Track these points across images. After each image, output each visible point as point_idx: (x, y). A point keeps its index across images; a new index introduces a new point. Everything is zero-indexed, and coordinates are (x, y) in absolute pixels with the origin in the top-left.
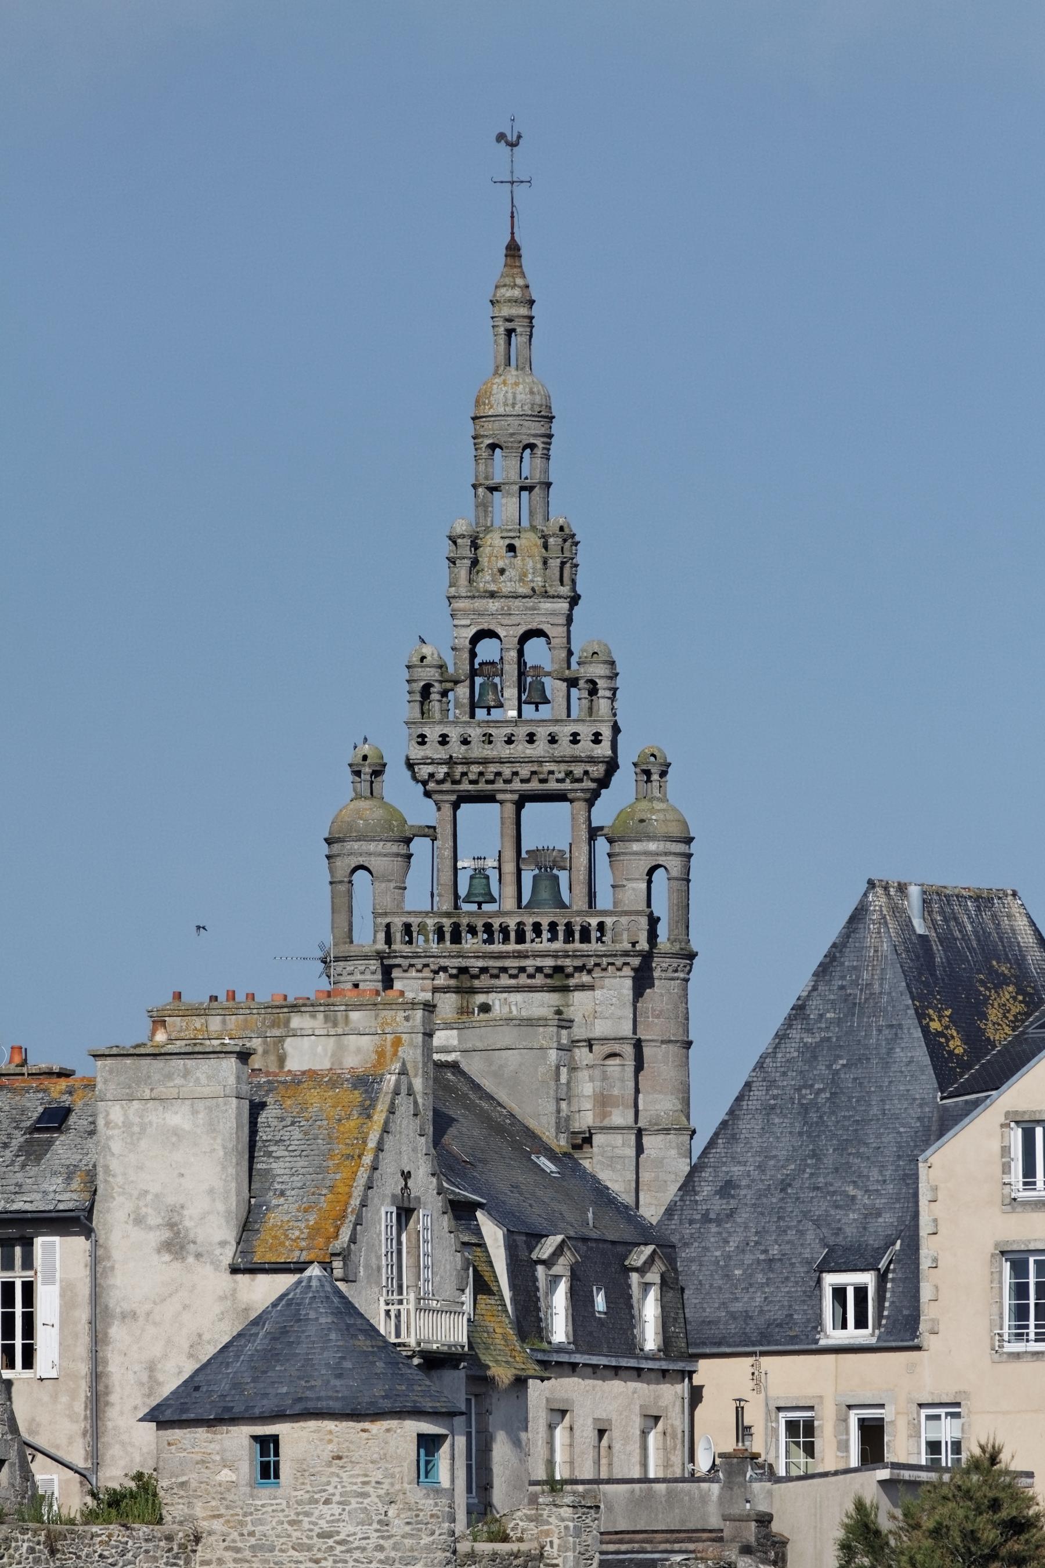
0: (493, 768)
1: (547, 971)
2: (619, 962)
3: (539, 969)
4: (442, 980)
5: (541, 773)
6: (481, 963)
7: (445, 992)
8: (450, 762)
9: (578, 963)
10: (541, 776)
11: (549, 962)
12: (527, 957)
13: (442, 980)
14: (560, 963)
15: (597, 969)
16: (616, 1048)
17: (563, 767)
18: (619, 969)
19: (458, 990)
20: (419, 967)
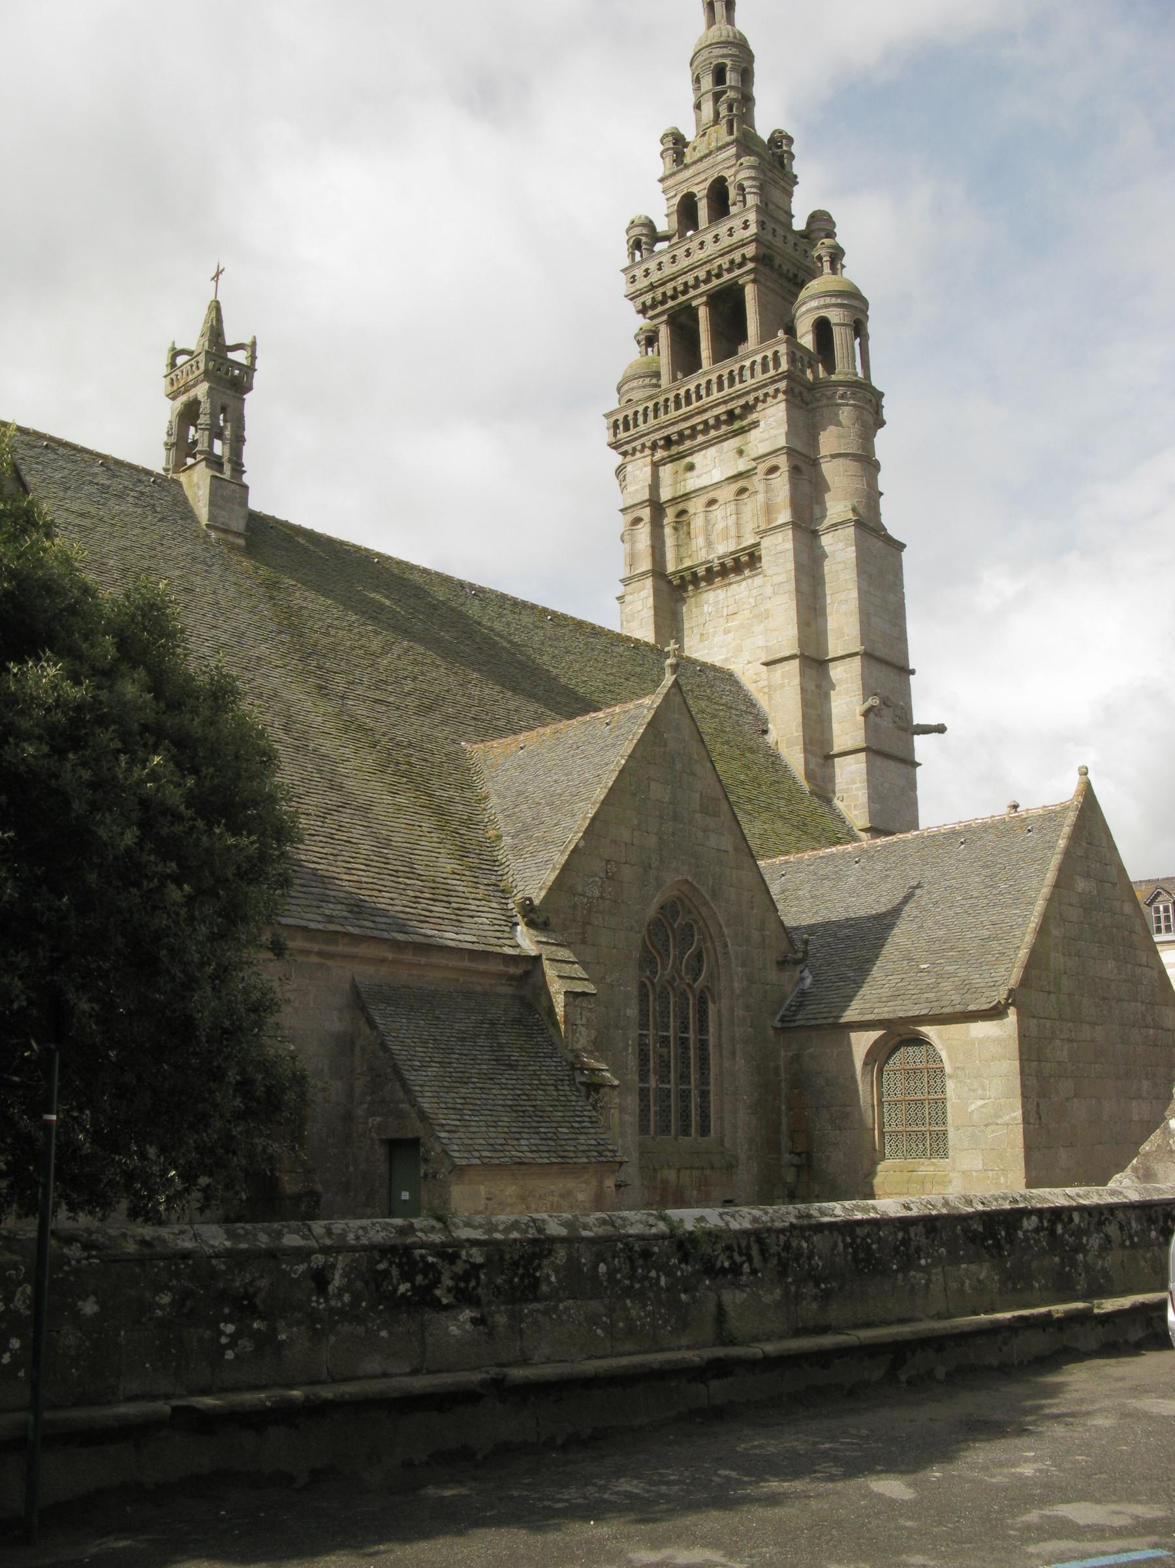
0: (681, 280)
1: (723, 418)
2: (770, 390)
3: (717, 418)
4: (660, 454)
5: (713, 270)
6: (676, 428)
7: (664, 464)
8: (652, 287)
9: (742, 402)
10: (713, 273)
11: (722, 409)
12: (705, 411)
13: (660, 454)
14: (730, 406)
15: (760, 404)
16: (773, 461)
17: (727, 258)
18: (775, 397)
19: (673, 459)
20: (639, 448)
